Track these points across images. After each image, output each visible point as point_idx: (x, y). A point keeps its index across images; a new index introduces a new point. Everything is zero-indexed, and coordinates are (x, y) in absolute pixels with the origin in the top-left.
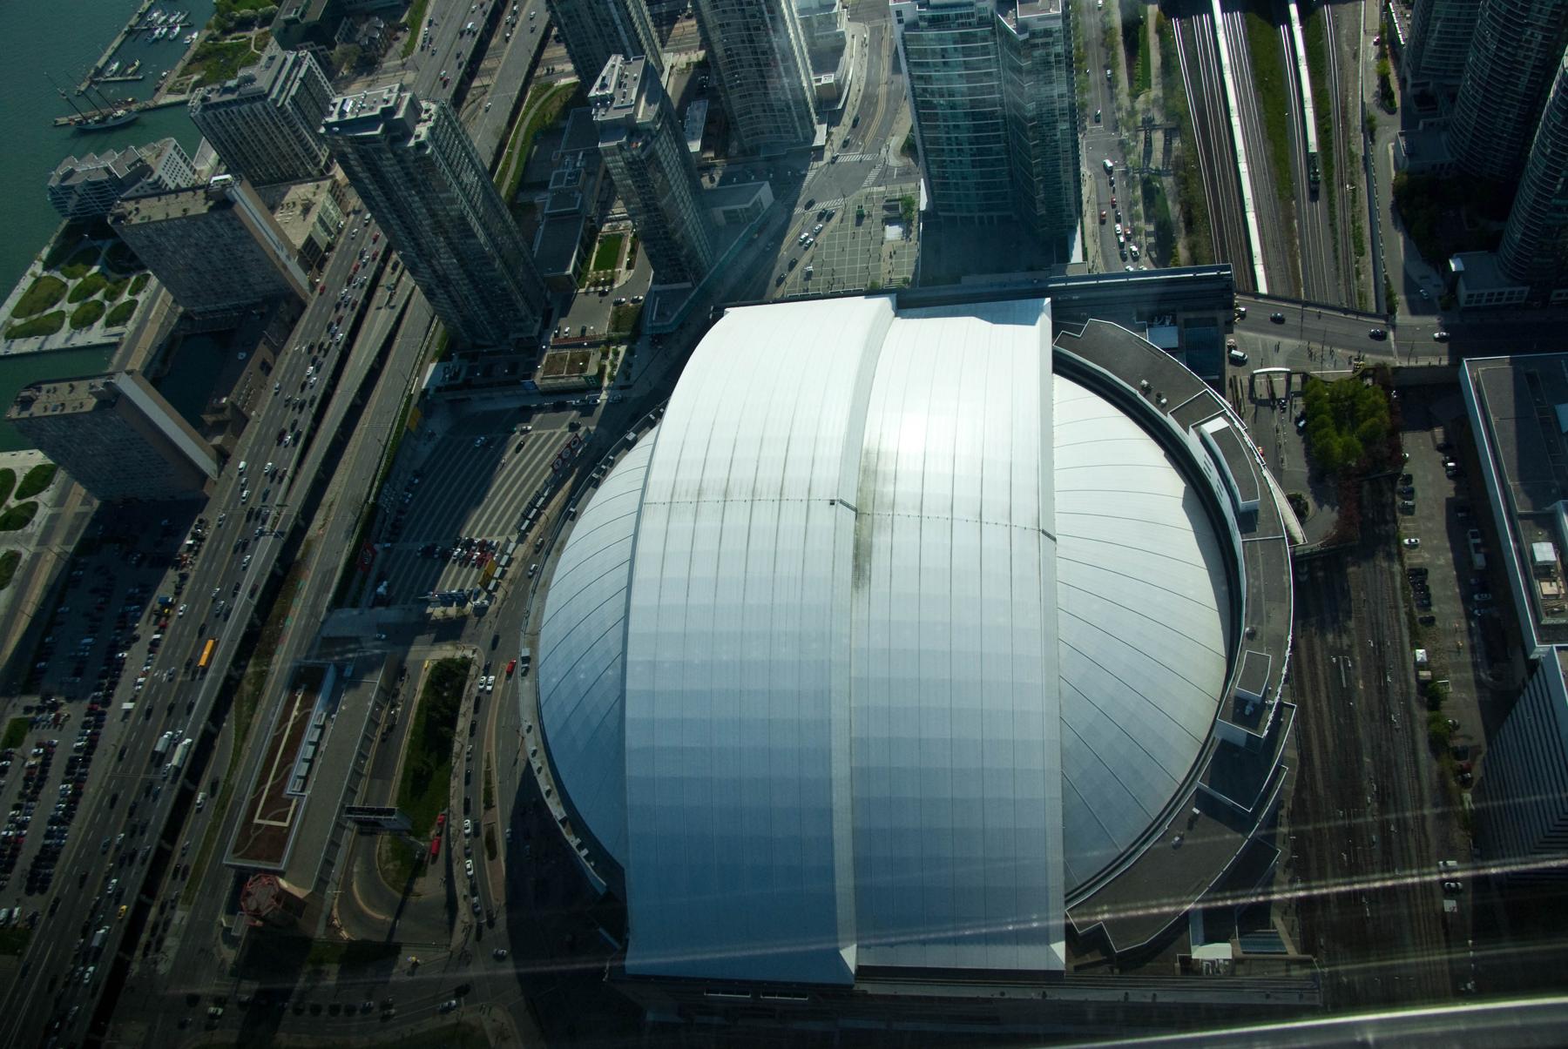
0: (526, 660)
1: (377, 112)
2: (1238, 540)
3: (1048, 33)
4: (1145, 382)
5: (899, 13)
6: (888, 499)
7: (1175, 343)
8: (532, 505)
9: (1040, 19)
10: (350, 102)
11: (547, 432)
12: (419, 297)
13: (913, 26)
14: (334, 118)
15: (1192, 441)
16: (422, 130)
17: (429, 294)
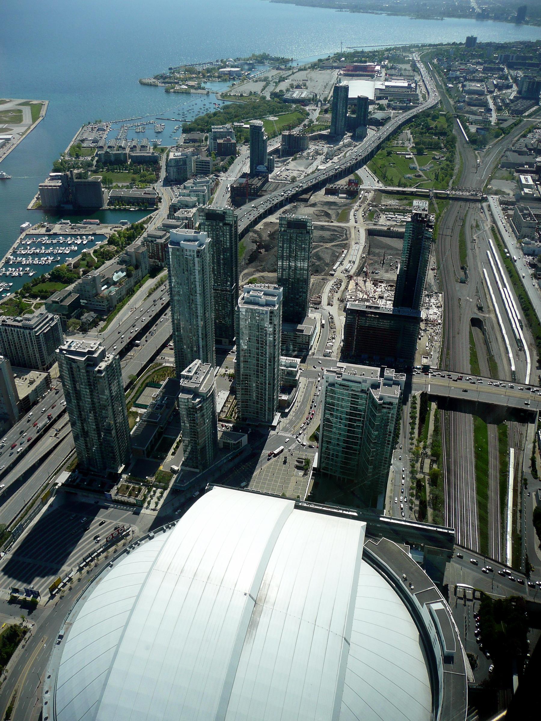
0: (61, 637)
1: (86, 351)
2: (441, 671)
3: (391, 404)
4: (404, 575)
5: (328, 378)
6: (272, 600)
7: (421, 561)
8: (90, 555)
9: (389, 397)
10: (74, 342)
11: (108, 521)
12: (70, 439)
13: (332, 385)
14: (65, 347)
15: (424, 612)
16: (103, 365)
17: (76, 438)
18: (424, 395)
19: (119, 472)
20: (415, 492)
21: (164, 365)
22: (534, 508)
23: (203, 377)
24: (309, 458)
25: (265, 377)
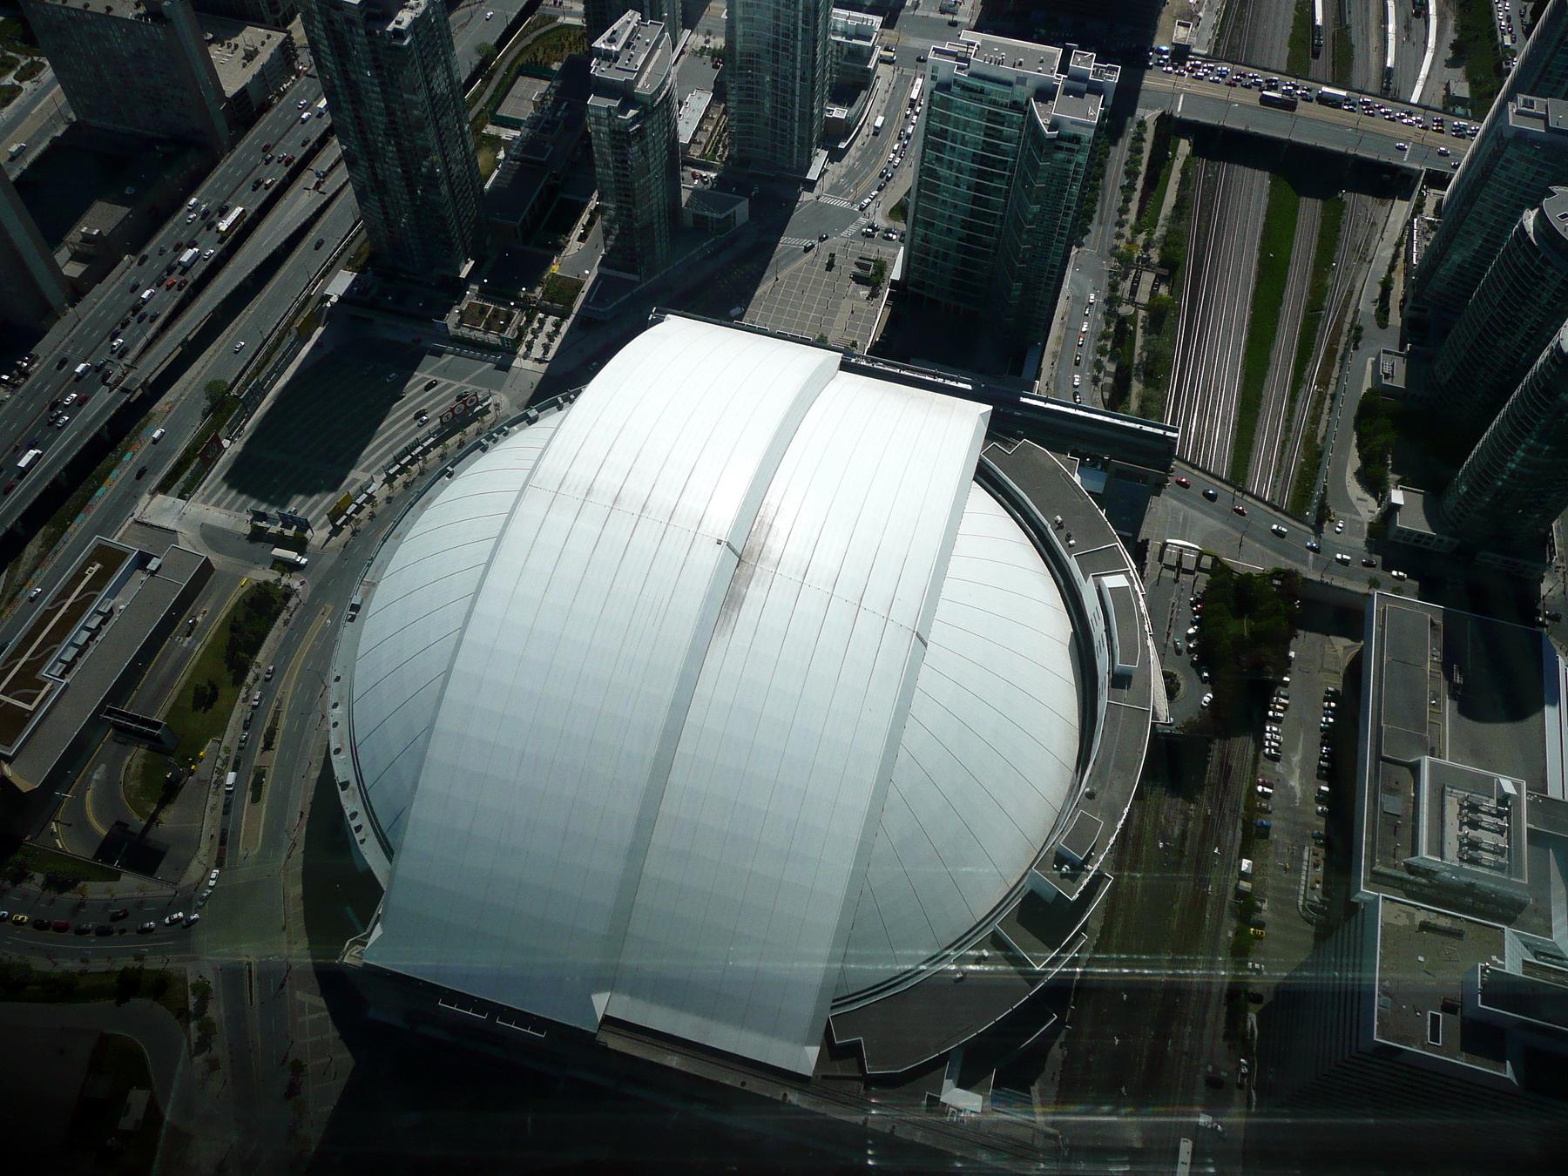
0: (356, 608)
3: (1076, 139)
4: (1059, 518)
5: (935, 69)
6: (775, 556)
8: (408, 451)
9: (1073, 122)
11: (444, 382)
13: (944, 87)
17: (361, 196)
18: (1165, 121)
19: (463, 275)
20: (1109, 344)
21: (560, 20)
22: (1364, 391)
23: (643, 56)
24: (885, 258)
25: (794, 60)
